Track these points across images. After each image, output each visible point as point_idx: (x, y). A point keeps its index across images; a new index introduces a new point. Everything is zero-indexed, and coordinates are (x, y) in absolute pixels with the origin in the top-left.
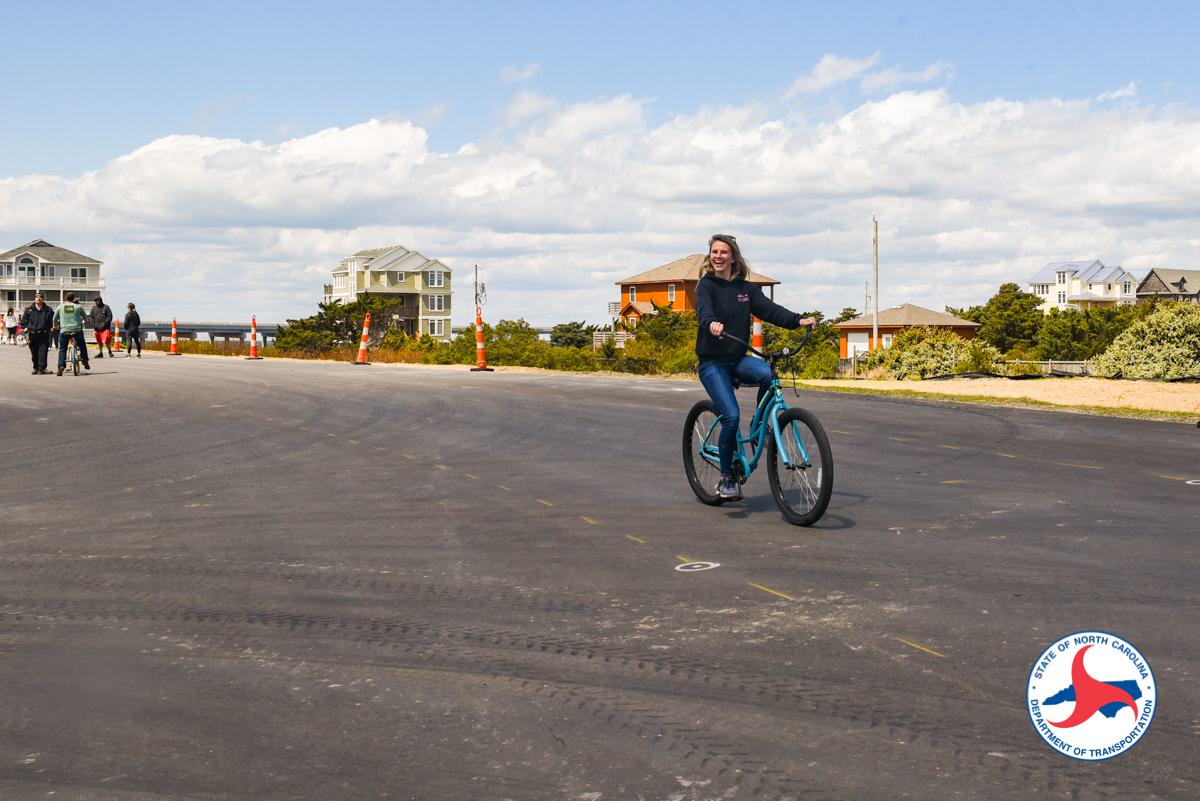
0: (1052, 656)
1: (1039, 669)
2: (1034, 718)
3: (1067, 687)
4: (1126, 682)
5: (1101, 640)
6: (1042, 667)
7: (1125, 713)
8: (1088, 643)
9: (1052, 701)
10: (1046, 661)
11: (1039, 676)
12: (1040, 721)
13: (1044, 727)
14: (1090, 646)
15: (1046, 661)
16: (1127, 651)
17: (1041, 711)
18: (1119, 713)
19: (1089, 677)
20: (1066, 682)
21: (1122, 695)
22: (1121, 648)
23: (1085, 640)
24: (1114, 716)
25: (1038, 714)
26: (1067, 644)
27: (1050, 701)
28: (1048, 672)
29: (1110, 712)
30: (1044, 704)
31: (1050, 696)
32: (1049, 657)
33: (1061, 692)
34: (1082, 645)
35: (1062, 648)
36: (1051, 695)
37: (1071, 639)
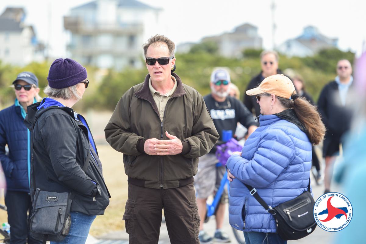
1: (317, 204)
2: (315, 219)
3: (326, 209)
4: (343, 208)
5: (336, 195)
6: (318, 203)
7: (343, 217)
8: (332, 196)
9: (321, 213)
10: (319, 201)
11: (317, 206)
12: (317, 220)
13: (318, 221)
14: (332, 197)
15: (319, 201)
17: (317, 217)
18: (341, 217)
19: (332, 206)
20: (325, 208)
21: (342, 212)
22: (342, 197)
23: (331, 195)
24: (340, 218)
25: (317, 218)
26: (325, 196)
27: (320, 214)
29: (339, 217)
30: (318, 214)
31: (320, 212)
32: (320, 200)
33: (324, 211)
34: (330, 197)
35: (324, 197)
36: (321, 212)
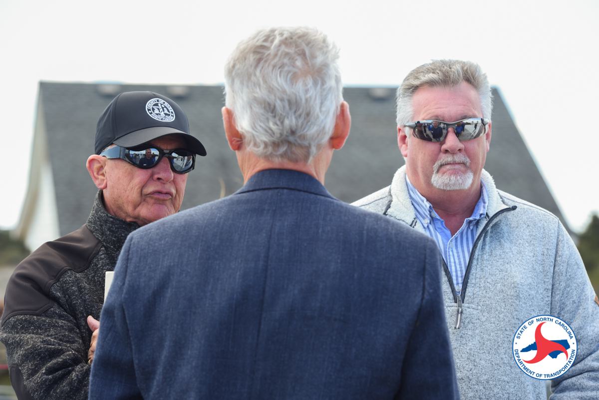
0: (525, 327)
1: (519, 334)
3: (533, 343)
4: (562, 341)
5: (549, 320)
6: (520, 333)
7: (562, 356)
8: (543, 321)
9: (525, 350)
10: (522, 330)
11: (519, 337)
12: (519, 360)
13: (521, 363)
14: (544, 323)
15: (522, 330)
16: (563, 325)
17: (520, 355)
18: (559, 356)
19: (544, 338)
20: (532, 340)
21: (560, 347)
22: (560, 323)
23: (541, 319)
24: (556, 357)
25: (518, 357)
26: (532, 322)
27: (524, 350)
28: (523, 336)
29: (554, 355)
30: (521, 351)
31: (524, 348)
32: (524, 328)
33: (529, 346)
34: (540, 322)
35: (530, 323)
36: (525, 347)
37: (534, 319)
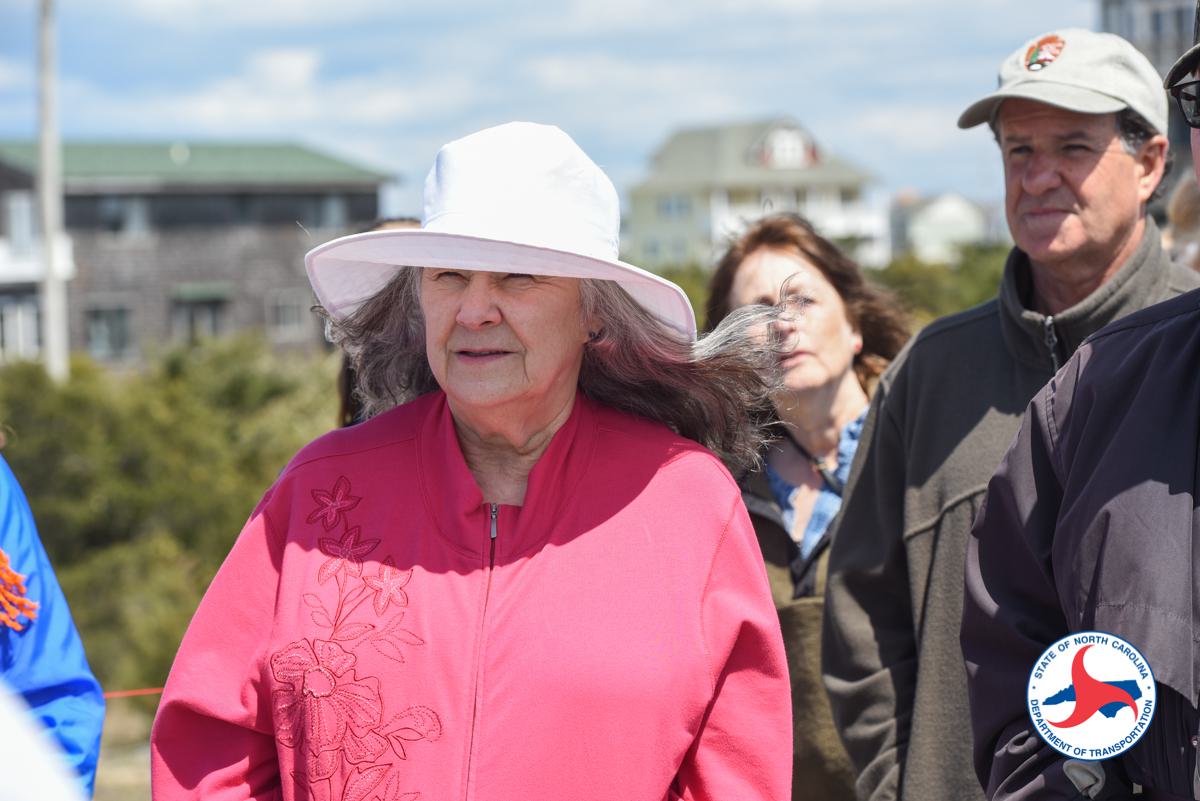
0: (1052, 656)
1: (1039, 669)
3: (1067, 687)
4: (1126, 682)
5: (1101, 640)
6: (1042, 667)
7: (1125, 713)
8: (1088, 643)
9: (1052, 701)
10: (1046, 661)
11: (1039, 676)
12: (1040, 721)
13: (1044, 727)
14: (1090, 646)
15: (1046, 661)
16: (1127, 651)
17: (1041, 711)
18: (1119, 713)
19: (1089, 677)
20: (1066, 682)
21: (1122, 695)
22: (1121, 648)
23: (1085, 640)
24: (1114, 716)
25: (1038, 714)
26: (1067, 644)
27: (1050, 701)
28: (1048, 672)
29: (1110, 712)
30: (1044, 704)
31: (1050, 696)
32: (1049, 657)
33: (1061, 692)
34: (1082, 645)
35: (1062, 648)
36: (1051, 695)
37: (1070, 639)
